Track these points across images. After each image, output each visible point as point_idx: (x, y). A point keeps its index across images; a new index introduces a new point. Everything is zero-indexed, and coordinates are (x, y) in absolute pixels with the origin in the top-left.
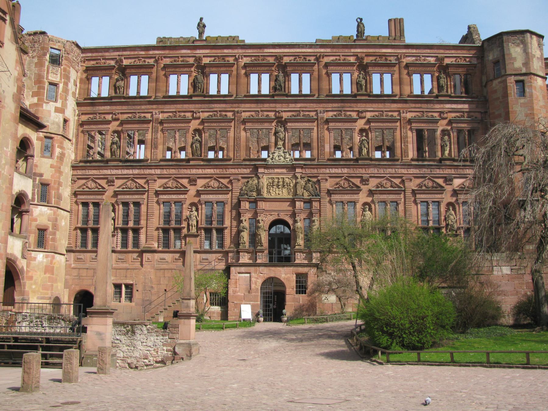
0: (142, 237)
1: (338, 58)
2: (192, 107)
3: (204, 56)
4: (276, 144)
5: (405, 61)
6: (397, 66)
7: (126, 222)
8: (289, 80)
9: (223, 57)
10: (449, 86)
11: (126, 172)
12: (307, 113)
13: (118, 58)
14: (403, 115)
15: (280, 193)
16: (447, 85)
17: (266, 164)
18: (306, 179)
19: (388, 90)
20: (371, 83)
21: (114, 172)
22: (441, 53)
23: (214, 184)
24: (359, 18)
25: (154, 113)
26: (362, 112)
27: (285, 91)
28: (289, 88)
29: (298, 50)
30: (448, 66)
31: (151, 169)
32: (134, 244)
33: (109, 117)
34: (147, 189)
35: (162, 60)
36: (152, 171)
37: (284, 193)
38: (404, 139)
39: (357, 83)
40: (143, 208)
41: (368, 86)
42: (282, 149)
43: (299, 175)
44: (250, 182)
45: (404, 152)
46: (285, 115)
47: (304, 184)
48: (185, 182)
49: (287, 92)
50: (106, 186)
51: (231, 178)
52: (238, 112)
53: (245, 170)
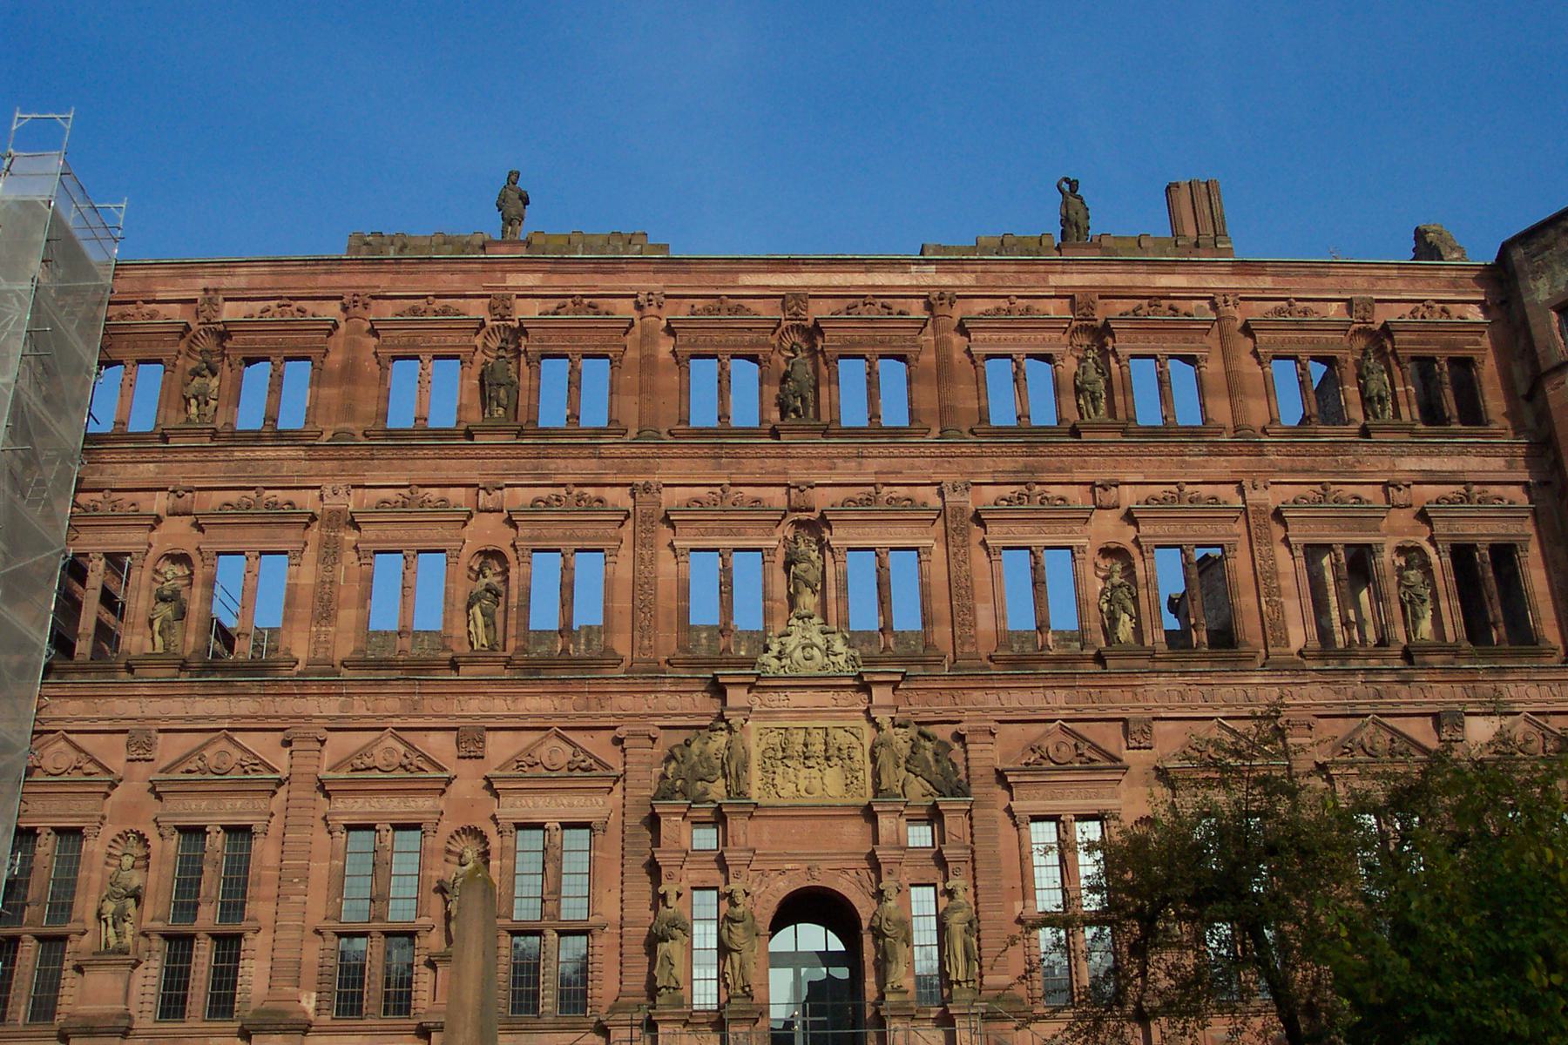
0: (254, 978)
1: (1004, 304)
2: (470, 471)
3: (518, 296)
4: (792, 600)
5: (1239, 315)
6: (1215, 333)
7: (186, 906)
8: (834, 380)
9: (588, 302)
10: (1402, 399)
11: (202, 706)
12: (902, 492)
13: (199, 295)
14: (1254, 497)
15: (817, 783)
16: (1394, 394)
17: (758, 677)
18: (913, 732)
19: (1187, 413)
20: (1127, 389)
21: (156, 707)
22: (1359, 287)
23: (556, 753)
24: (1067, 180)
25: (328, 492)
26: (1105, 487)
27: (817, 416)
28: (835, 407)
29: (860, 279)
30: (1386, 330)
31: (304, 695)
32: (215, 999)
33: (160, 503)
34: (284, 774)
35: (366, 306)
36: (310, 706)
37: (830, 784)
38: (1264, 580)
39: (1078, 391)
40: (264, 852)
41: (1119, 399)
42: (817, 620)
43: (883, 717)
44: (696, 747)
45: (1273, 629)
46: (823, 499)
47: (906, 752)
48: (440, 746)
49: (825, 418)
50: (118, 764)
51: (622, 732)
52: (647, 488)
53: (672, 701)
